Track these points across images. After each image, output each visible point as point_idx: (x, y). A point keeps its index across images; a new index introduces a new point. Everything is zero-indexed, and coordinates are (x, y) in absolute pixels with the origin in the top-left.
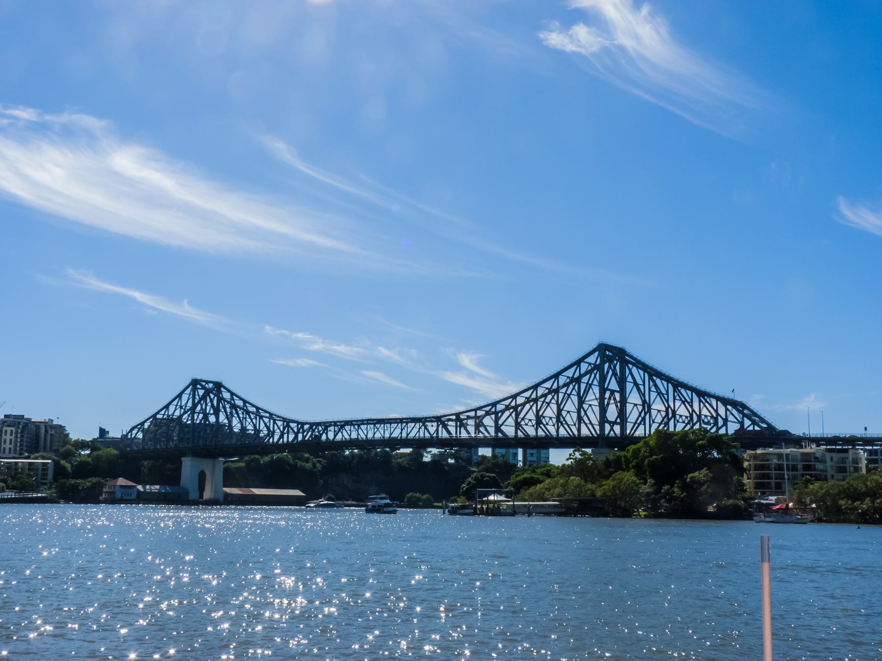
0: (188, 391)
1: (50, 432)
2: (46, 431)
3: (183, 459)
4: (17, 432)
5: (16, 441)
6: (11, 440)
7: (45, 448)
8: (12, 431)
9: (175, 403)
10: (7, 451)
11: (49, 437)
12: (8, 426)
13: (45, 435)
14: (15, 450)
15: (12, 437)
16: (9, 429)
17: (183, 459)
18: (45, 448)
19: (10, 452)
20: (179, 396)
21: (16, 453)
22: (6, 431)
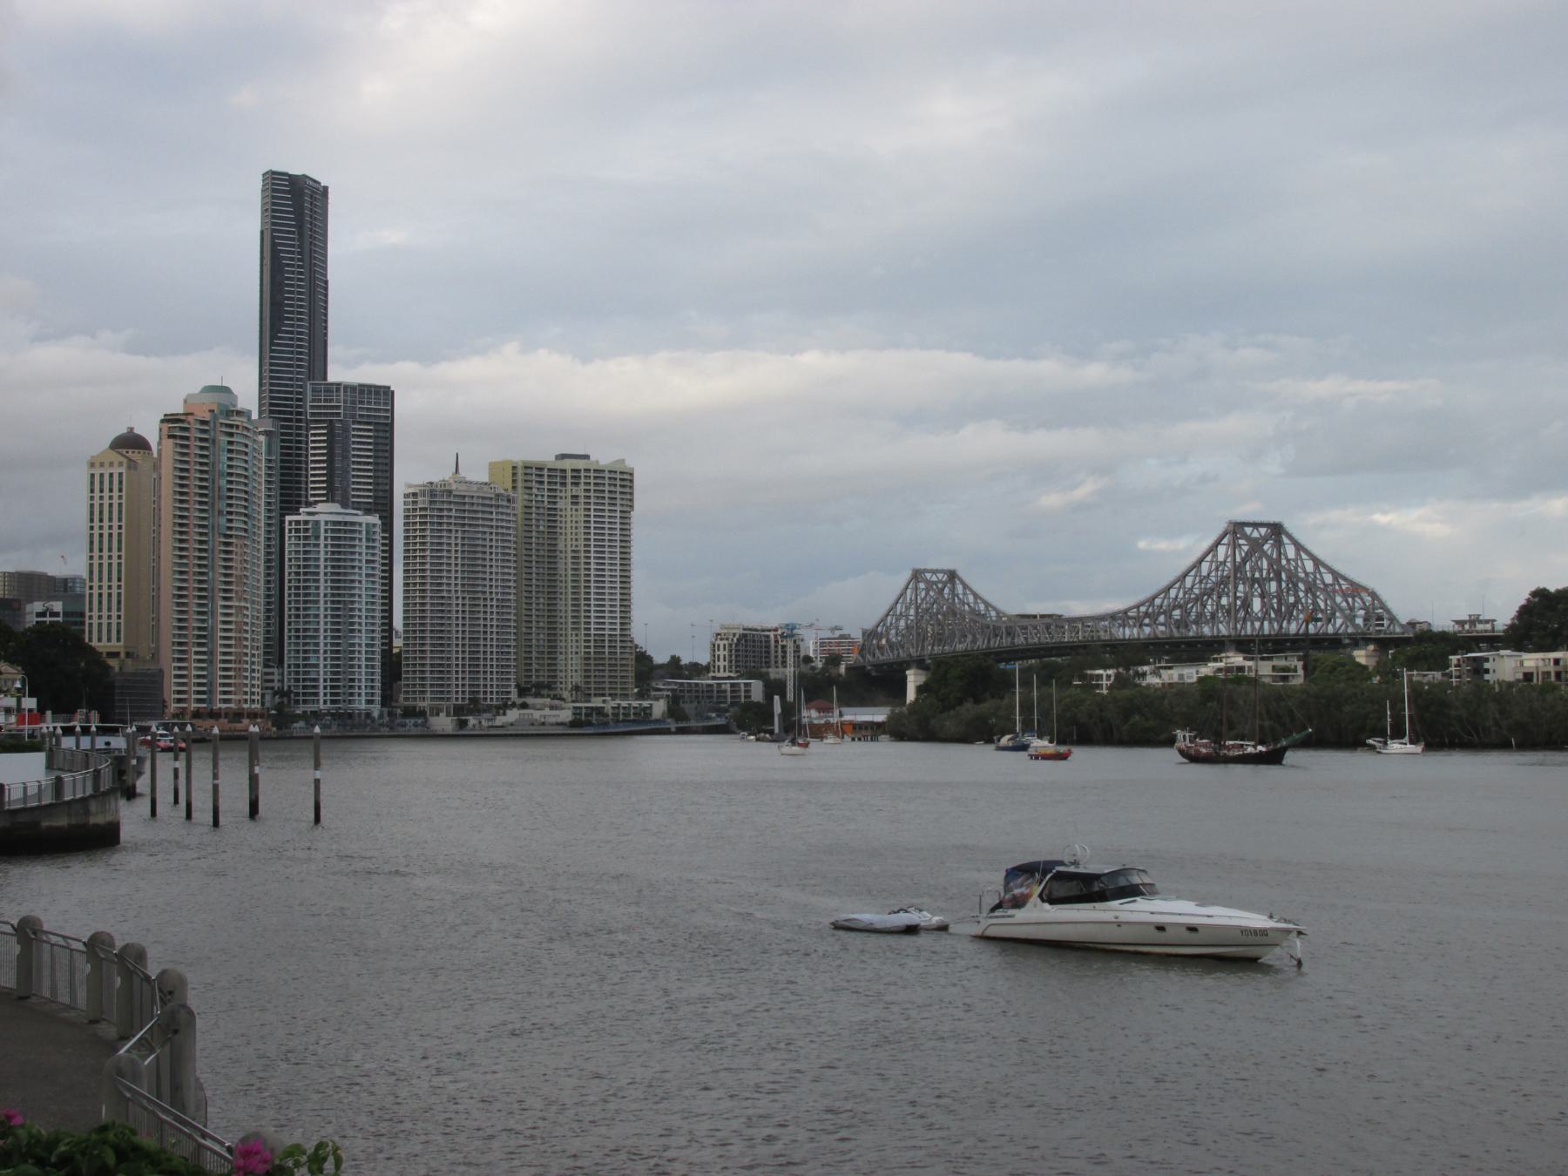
0: (910, 587)
1: (780, 643)
2: (777, 641)
3: (907, 672)
4: (730, 645)
5: (730, 656)
6: (725, 656)
7: (776, 662)
8: (725, 645)
9: (900, 601)
10: (722, 670)
11: (780, 647)
12: (721, 639)
13: (776, 647)
14: (730, 667)
15: (726, 653)
16: (722, 643)
17: (907, 672)
18: (776, 662)
19: (725, 671)
20: (903, 594)
21: (731, 672)
22: (719, 646)
